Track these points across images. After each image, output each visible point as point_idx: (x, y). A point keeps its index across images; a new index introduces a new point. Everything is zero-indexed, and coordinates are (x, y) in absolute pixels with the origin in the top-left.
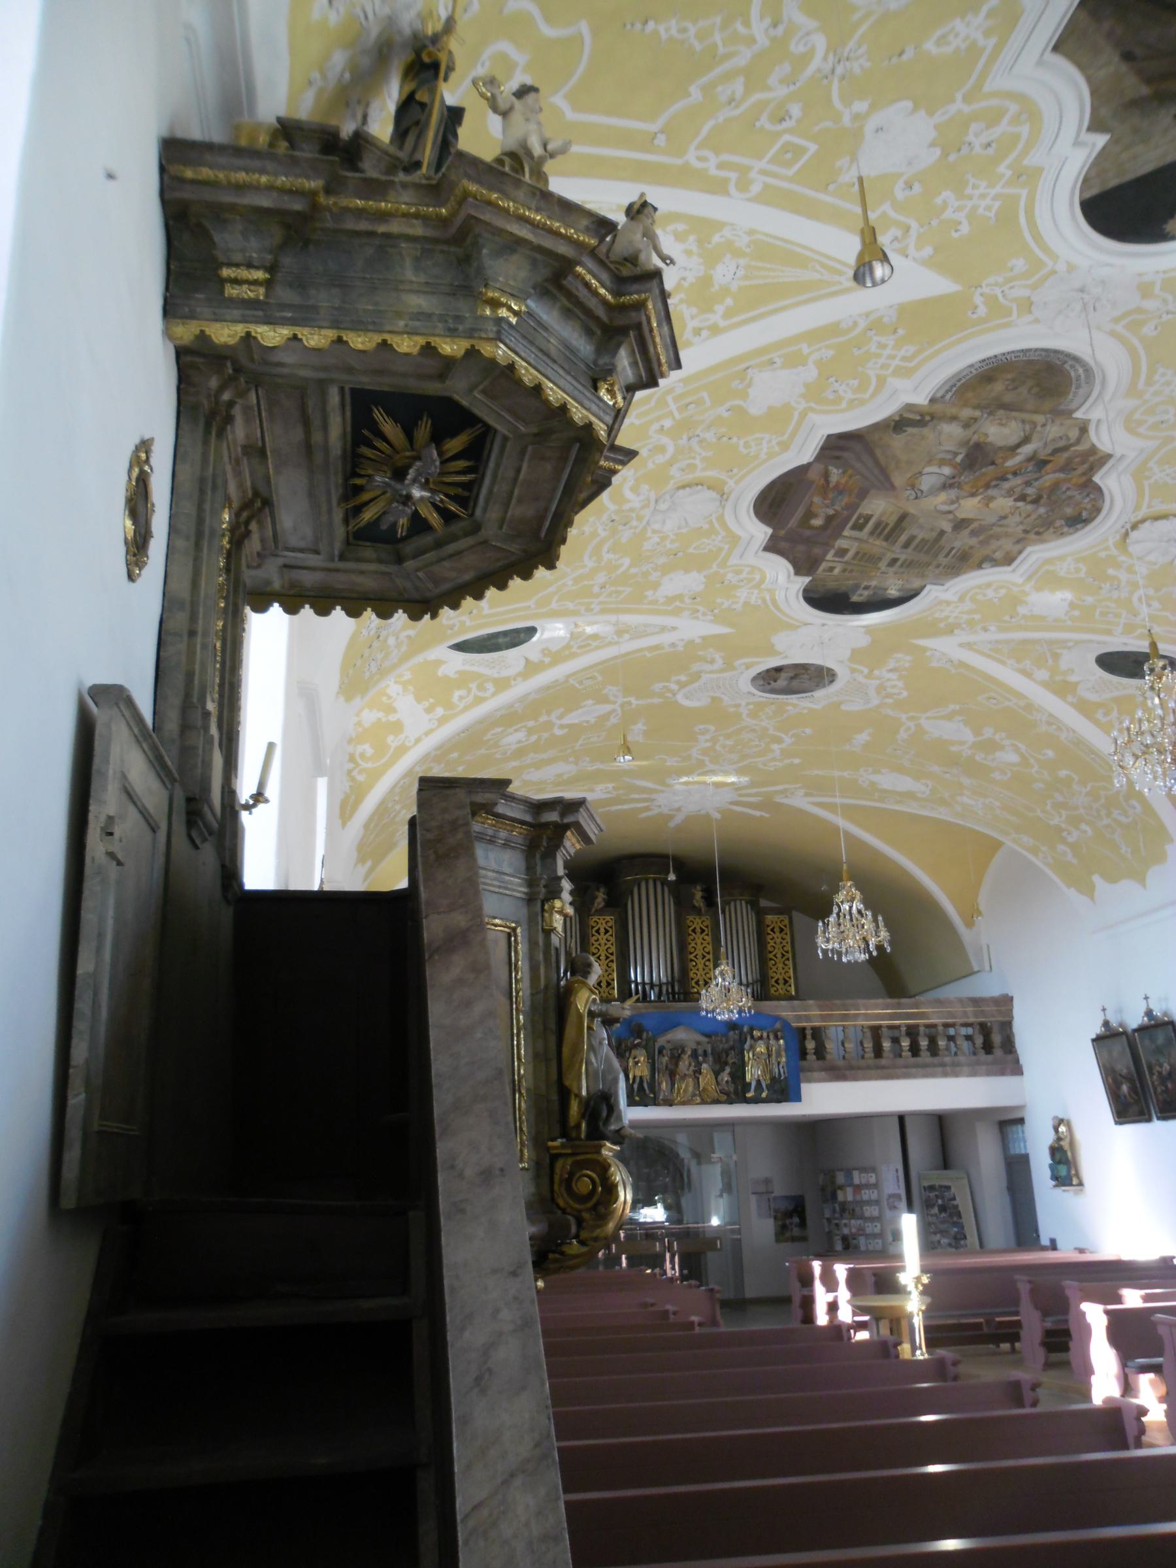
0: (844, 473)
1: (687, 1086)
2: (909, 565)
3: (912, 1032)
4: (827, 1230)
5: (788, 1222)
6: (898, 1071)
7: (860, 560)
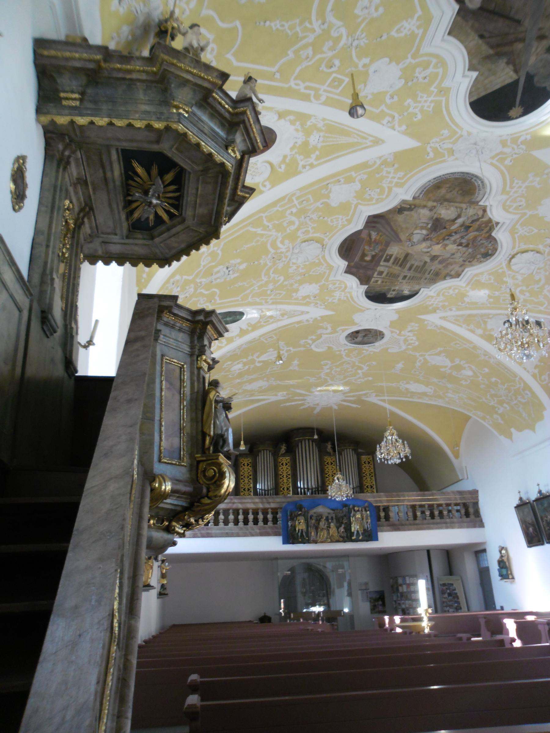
0: (378, 234)
1: (323, 535)
2: (412, 278)
3: (431, 507)
4: (395, 606)
5: (376, 604)
6: (425, 526)
7: (390, 277)
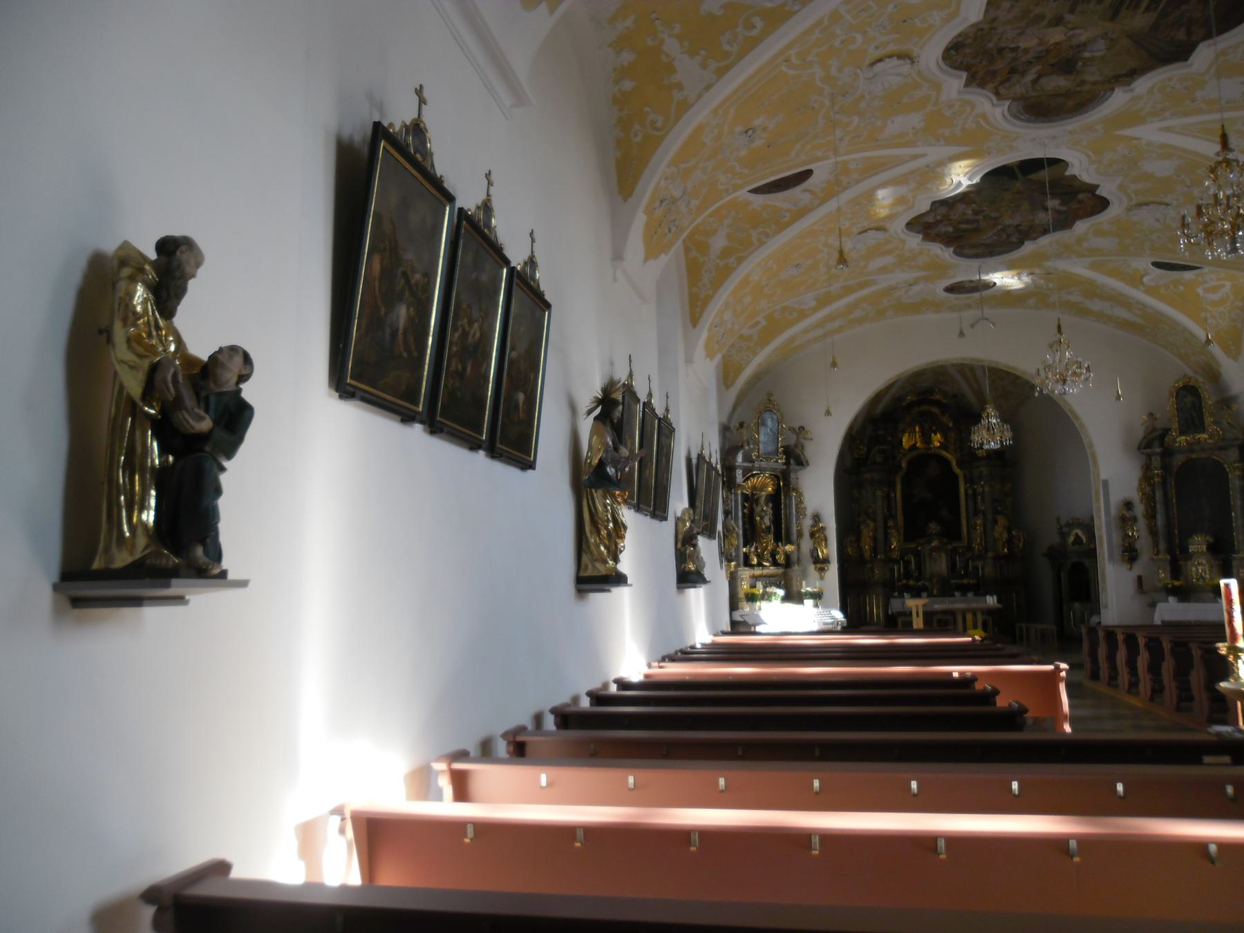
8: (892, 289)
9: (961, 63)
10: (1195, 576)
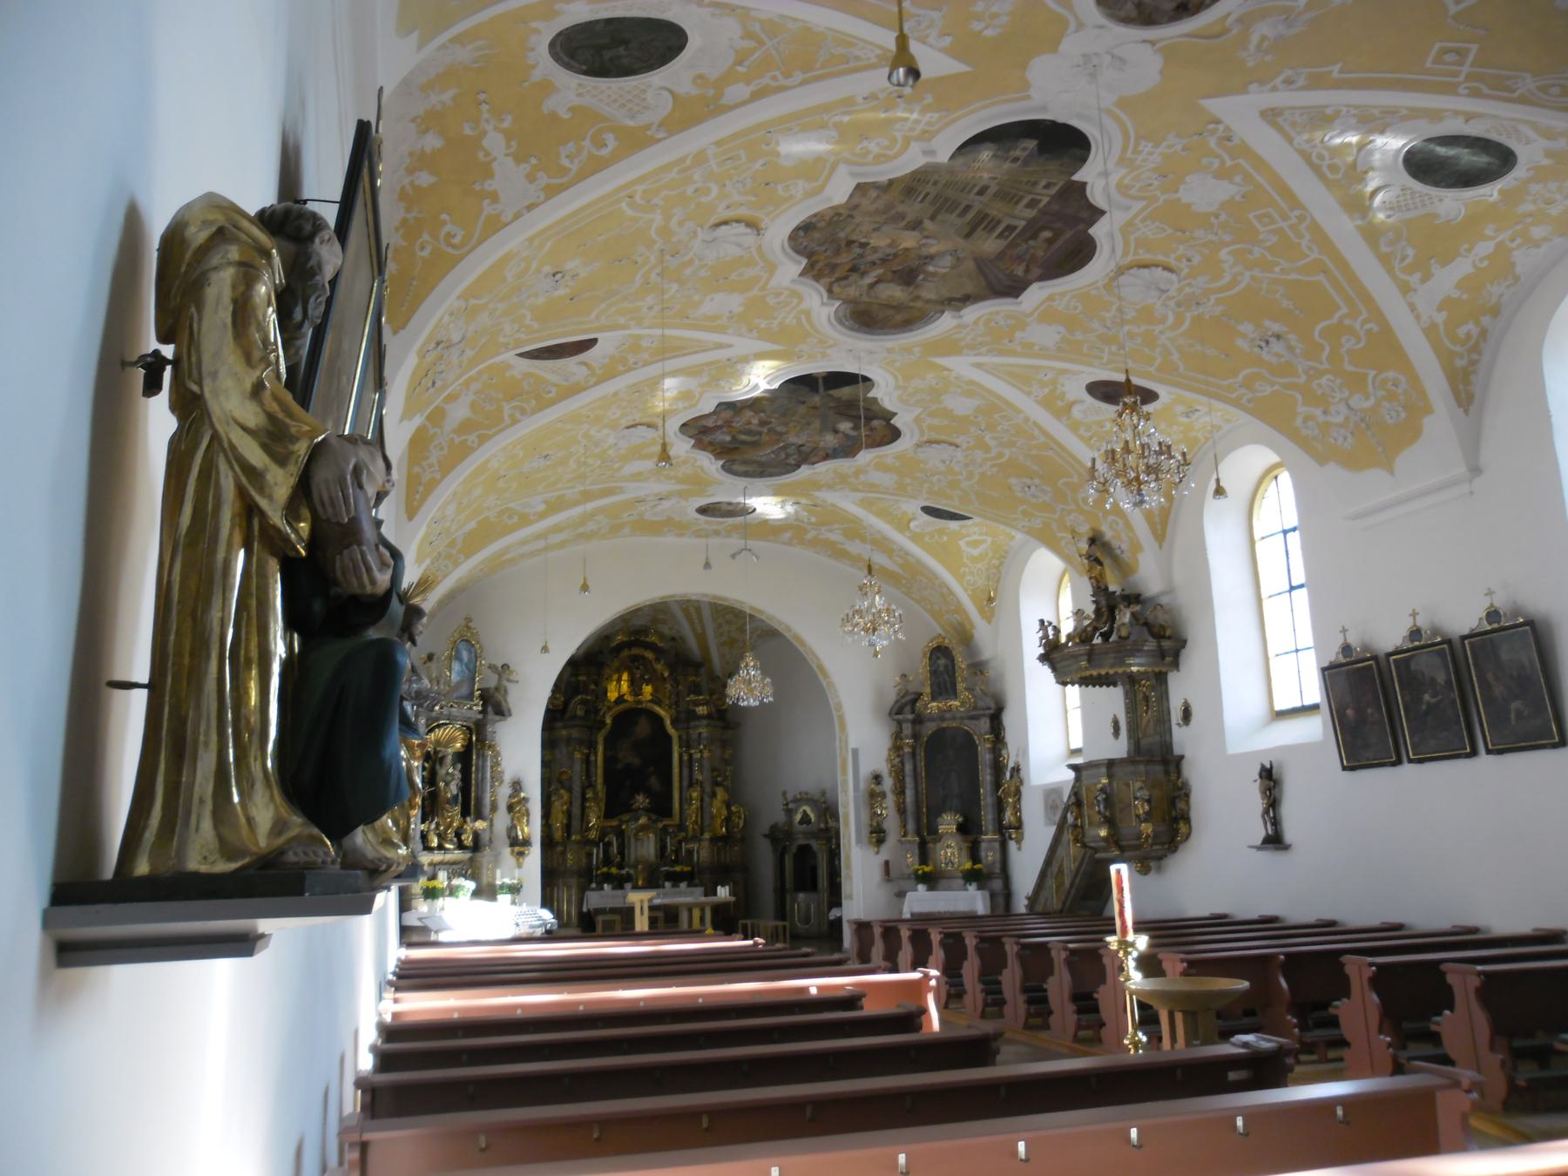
0: (1013, 271)
2: (965, 188)
7: (1016, 195)
8: (640, 501)
9: (805, 247)
10: (944, 861)
